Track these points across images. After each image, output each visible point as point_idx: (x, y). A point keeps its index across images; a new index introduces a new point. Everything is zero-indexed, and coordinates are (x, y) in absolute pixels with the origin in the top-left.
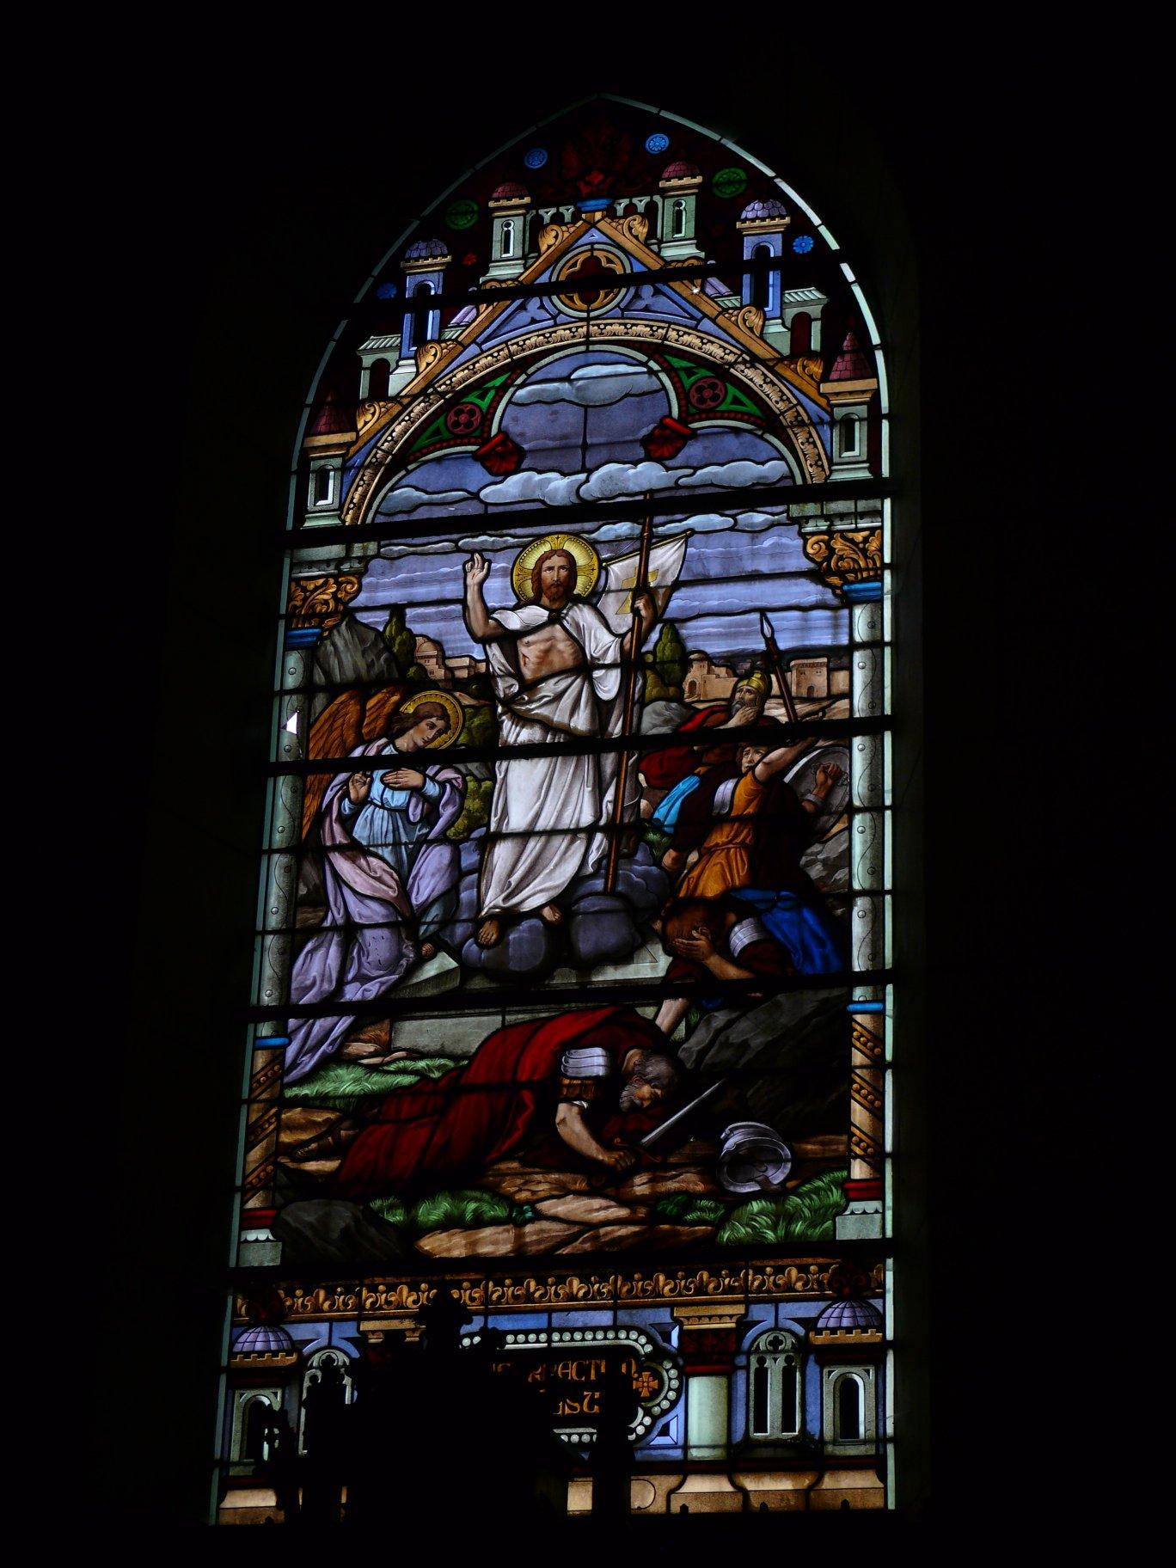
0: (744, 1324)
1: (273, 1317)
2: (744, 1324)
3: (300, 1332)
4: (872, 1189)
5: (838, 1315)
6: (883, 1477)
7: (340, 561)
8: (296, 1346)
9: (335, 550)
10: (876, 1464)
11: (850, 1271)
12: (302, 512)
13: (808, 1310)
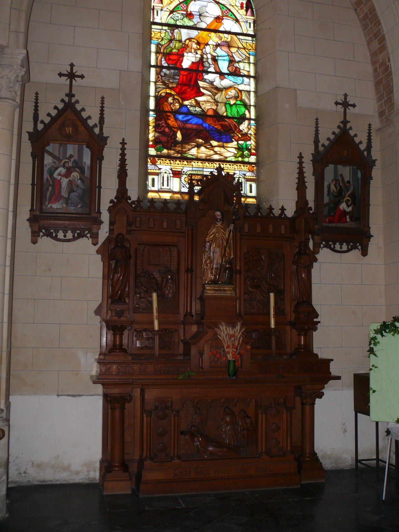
0: (235, 174)
1: (154, 163)
2: (235, 174)
3: (160, 167)
7: (160, 30)
8: (160, 169)
9: (160, 27)
12: (154, 18)
13: (245, 173)
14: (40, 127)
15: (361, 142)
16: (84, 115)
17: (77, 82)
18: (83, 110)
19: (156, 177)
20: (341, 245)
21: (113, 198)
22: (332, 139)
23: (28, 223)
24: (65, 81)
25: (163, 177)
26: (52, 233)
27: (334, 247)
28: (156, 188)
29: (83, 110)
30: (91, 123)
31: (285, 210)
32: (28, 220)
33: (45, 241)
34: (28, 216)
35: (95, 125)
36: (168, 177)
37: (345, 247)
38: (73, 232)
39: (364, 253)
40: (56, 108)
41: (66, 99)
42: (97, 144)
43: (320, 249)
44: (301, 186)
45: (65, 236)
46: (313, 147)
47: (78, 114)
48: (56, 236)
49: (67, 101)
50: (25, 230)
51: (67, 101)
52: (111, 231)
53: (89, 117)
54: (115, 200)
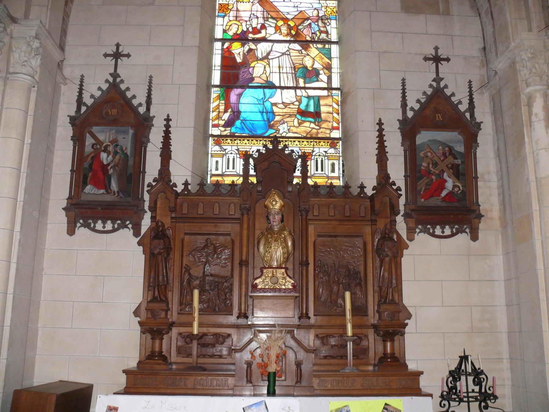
2: (313, 151)
3: (225, 147)
4: (337, 128)
5: (332, 151)
6: (340, 180)
8: (225, 150)
10: (338, 178)
11: (333, 142)
13: (326, 150)
14: (83, 109)
15: (460, 102)
16: (129, 94)
17: (123, 62)
18: (128, 89)
19: (220, 160)
20: (443, 228)
21: (152, 182)
22: (423, 101)
23: (64, 213)
24: (111, 61)
25: (228, 159)
26: (90, 223)
27: (434, 232)
28: (219, 172)
29: (128, 89)
30: (135, 102)
31: (365, 187)
32: (63, 209)
33: (82, 232)
34: (64, 204)
35: (140, 105)
36: (234, 159)
37: (447, 231)
38: (113, 223)
39: (474, 237)
40: (100, 89)
41: (111, 80)
42: (143, 124)
43: (416, 235)
44: (382, 158)
45: (104, 227)
46: (400, 111)
47: (122, 94)
48: (95, 226)
49: (111, 81)
50: (57, 218)
51: (111, 81)
52: (153, 218)
53: (134, 97)
54: (154, 184)
